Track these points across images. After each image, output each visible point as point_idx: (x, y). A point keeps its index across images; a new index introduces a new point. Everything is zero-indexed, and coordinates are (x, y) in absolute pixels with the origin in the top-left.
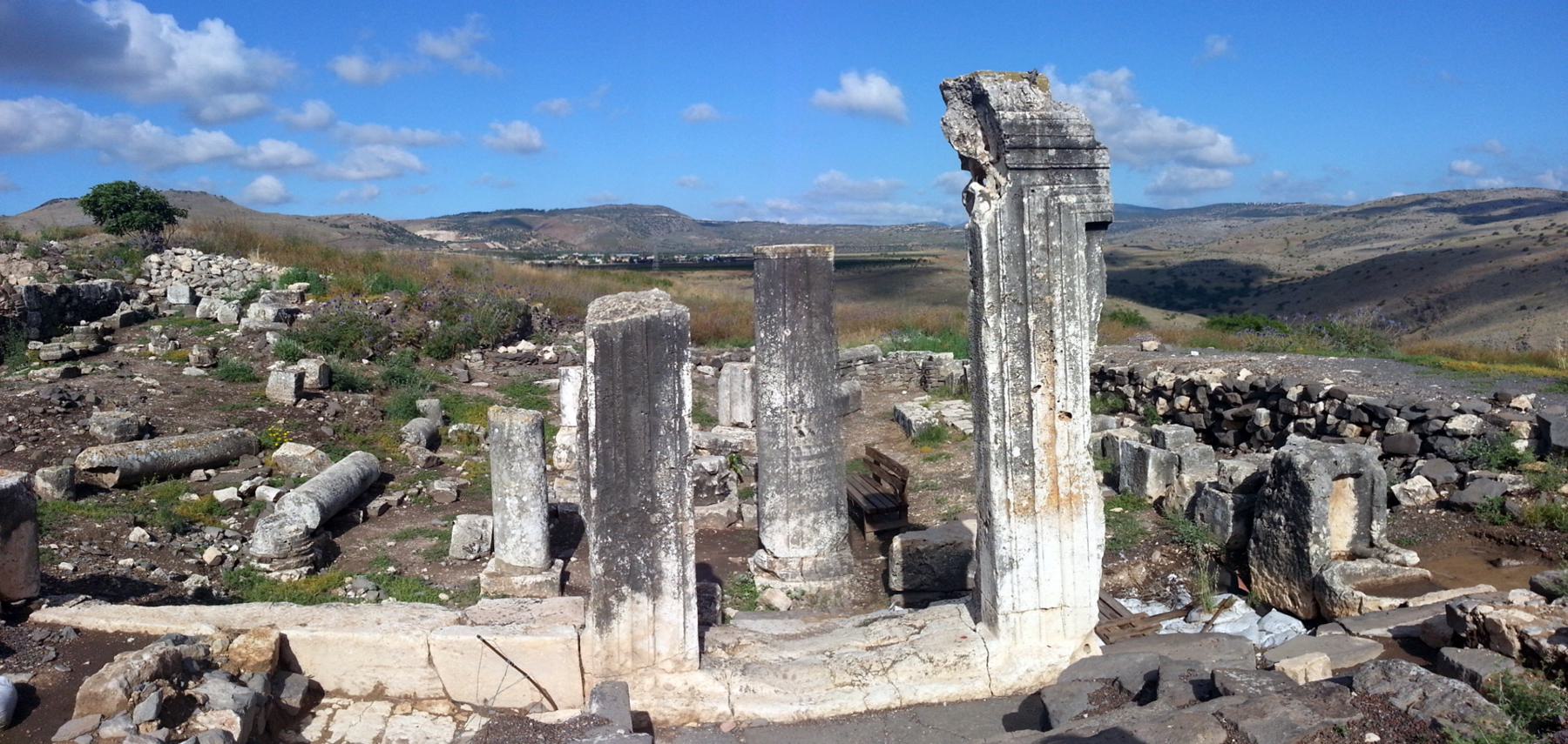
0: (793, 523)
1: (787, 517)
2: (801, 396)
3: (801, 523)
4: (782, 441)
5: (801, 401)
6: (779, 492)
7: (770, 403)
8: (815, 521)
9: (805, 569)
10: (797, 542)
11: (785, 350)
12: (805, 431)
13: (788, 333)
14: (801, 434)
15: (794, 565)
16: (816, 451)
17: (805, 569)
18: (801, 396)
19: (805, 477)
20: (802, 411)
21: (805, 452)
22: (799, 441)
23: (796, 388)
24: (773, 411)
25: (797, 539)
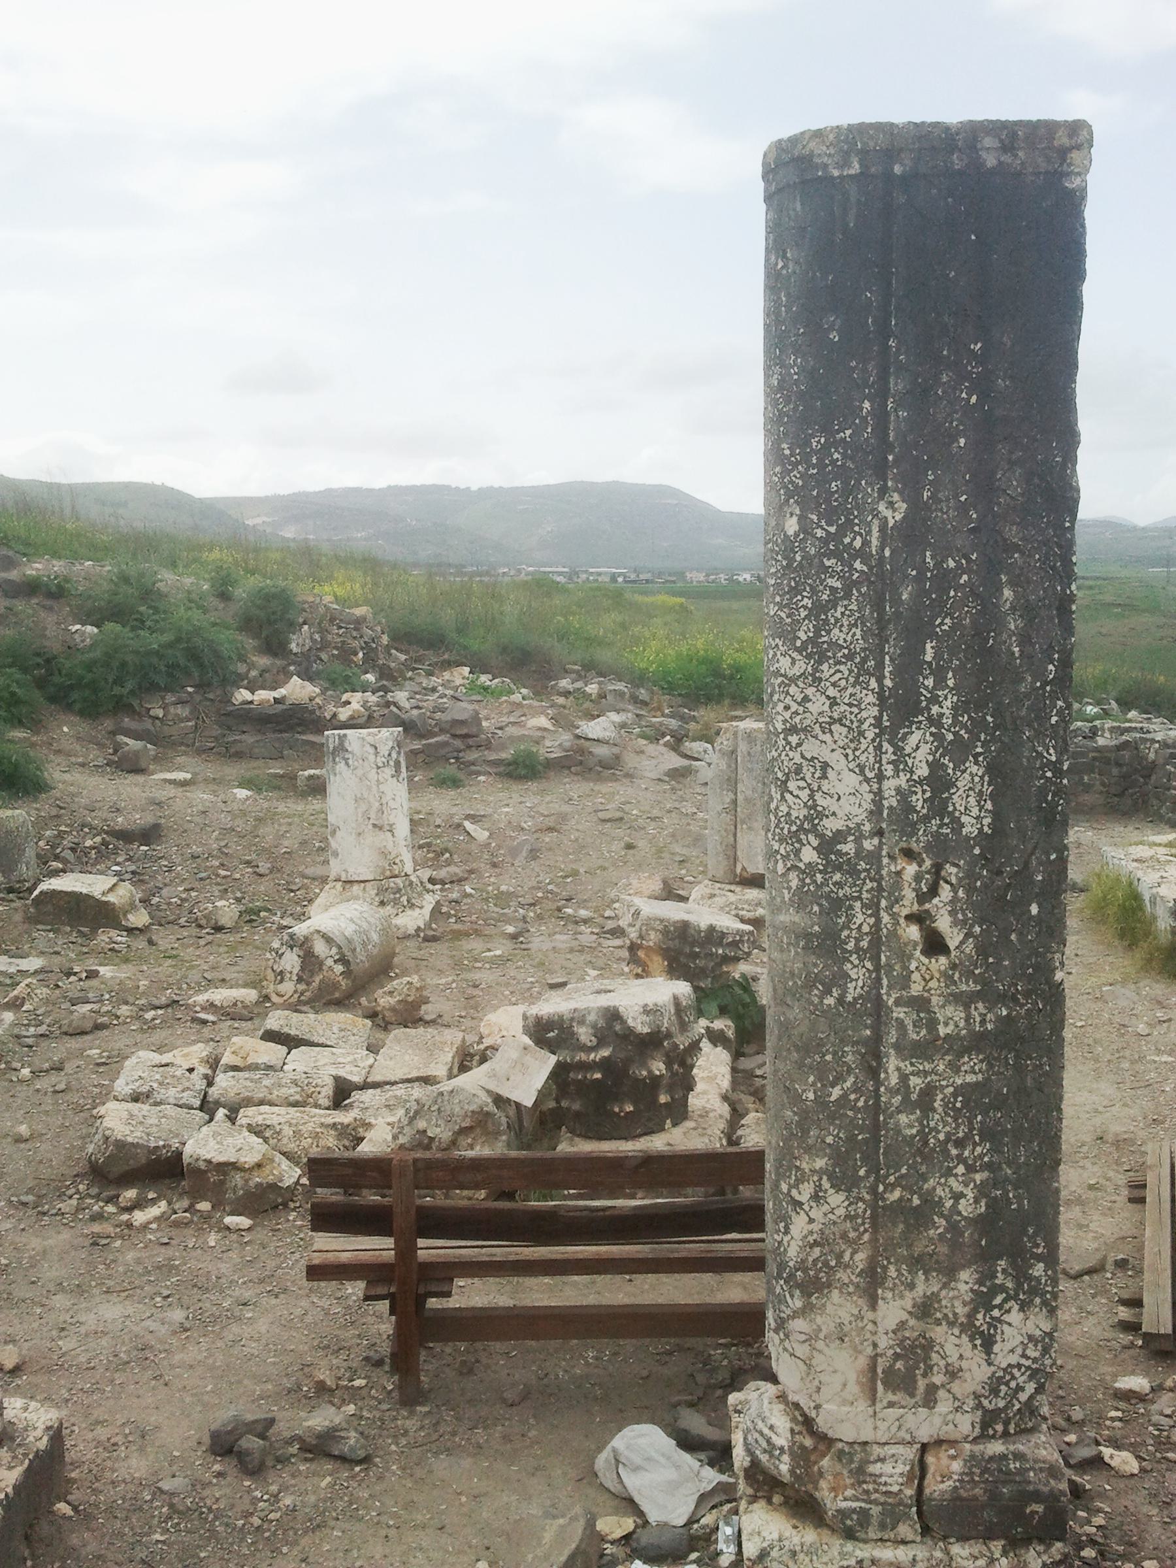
0: (893, 1311)
1: (872, 1285)
2: (939, 783)
3: (925, 1310)
4: (858, 974)
5: (939, 807)
6: (843, 1180)
7: (816, 814)
8: (982, 1301)
9: (936, 1487)
10: (900, 1382)
11: (880, 585)
12: (953, 938)
13: (894, 512)
14: (935, 945)
15: (892, 1472)
16: (985, 1017)
17: (936, 1487)
18: (939, 783)
19: (942, 1126)
20: (942, 850)
21: (951, 1020)
22: (927, 974)
23: (920, 746)
24: (827, 846)
25: (903, 1372)
